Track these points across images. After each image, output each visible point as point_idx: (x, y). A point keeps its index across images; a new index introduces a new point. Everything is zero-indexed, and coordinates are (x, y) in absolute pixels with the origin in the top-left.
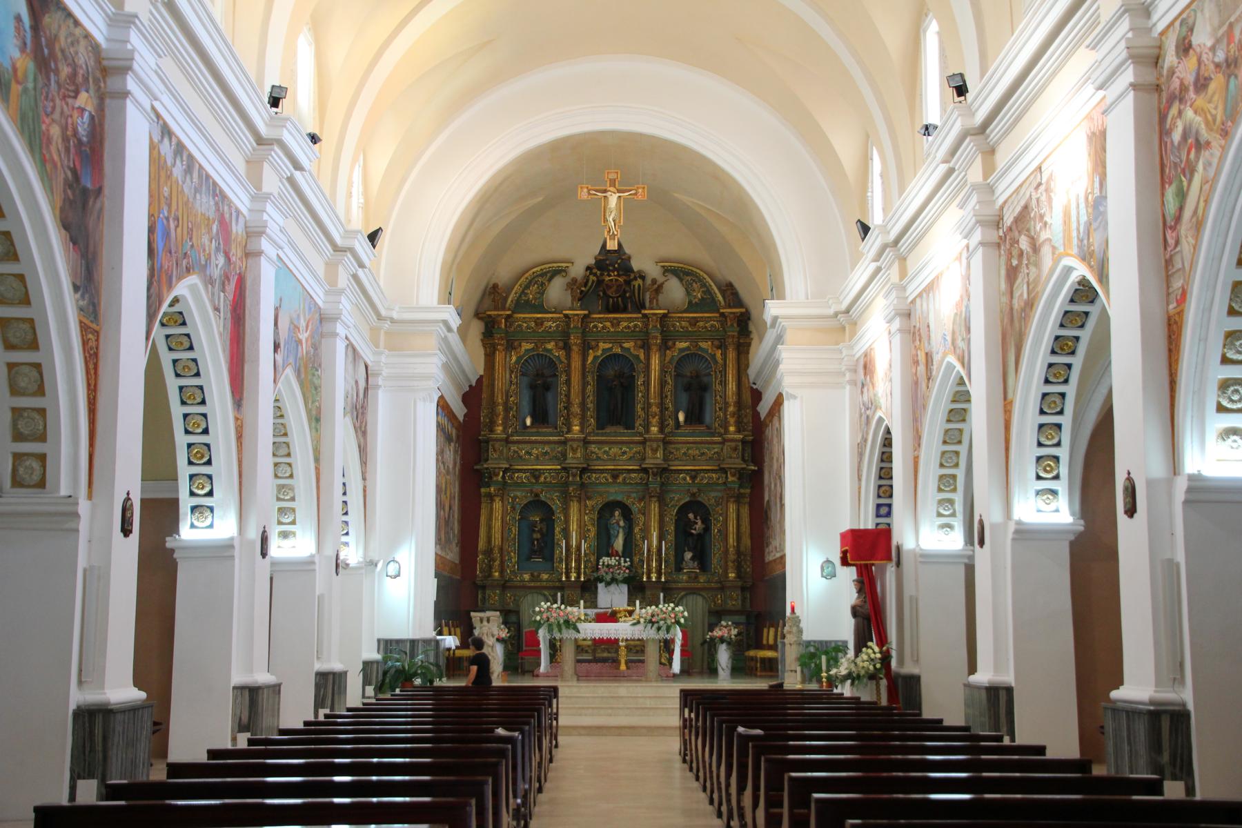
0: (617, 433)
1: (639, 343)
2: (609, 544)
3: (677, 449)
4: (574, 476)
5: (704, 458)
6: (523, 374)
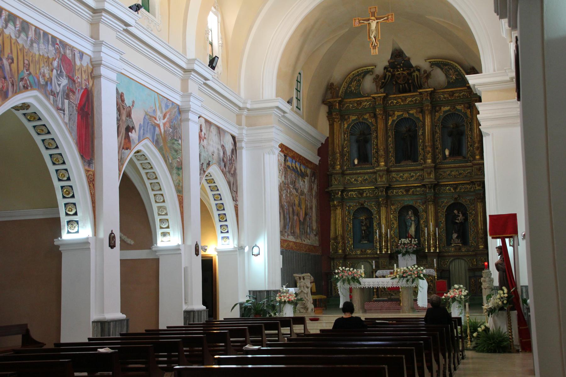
0: (408, 165)
1: (419, 110)
2: (407, 231)
3: (444, 172)
4: (382, 192)
5: (461, 176)
6: (352, 134)
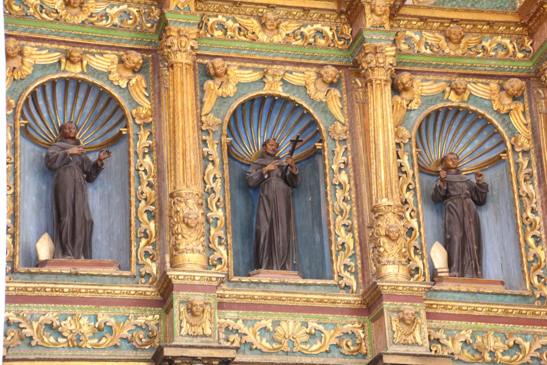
3: (446, 331)
